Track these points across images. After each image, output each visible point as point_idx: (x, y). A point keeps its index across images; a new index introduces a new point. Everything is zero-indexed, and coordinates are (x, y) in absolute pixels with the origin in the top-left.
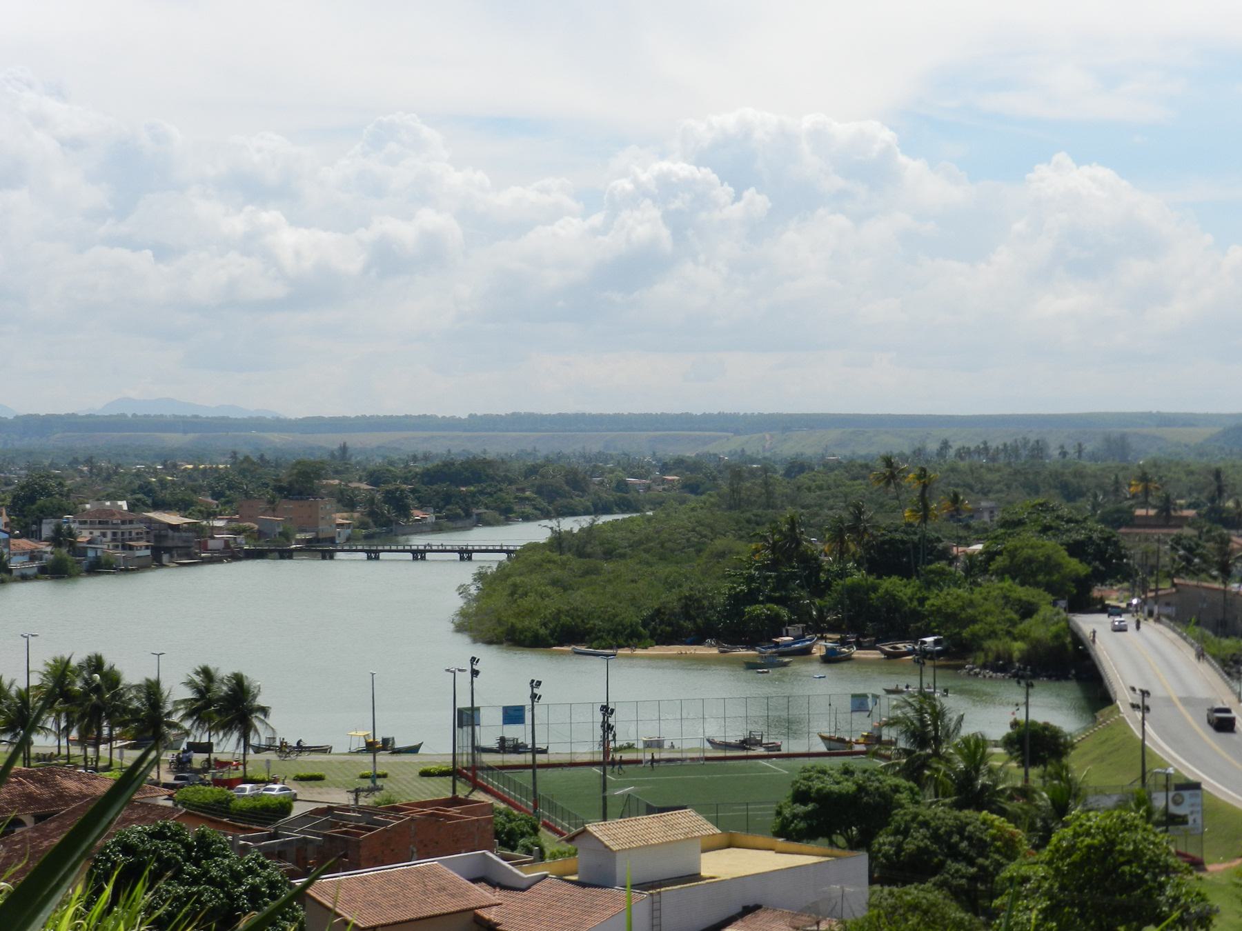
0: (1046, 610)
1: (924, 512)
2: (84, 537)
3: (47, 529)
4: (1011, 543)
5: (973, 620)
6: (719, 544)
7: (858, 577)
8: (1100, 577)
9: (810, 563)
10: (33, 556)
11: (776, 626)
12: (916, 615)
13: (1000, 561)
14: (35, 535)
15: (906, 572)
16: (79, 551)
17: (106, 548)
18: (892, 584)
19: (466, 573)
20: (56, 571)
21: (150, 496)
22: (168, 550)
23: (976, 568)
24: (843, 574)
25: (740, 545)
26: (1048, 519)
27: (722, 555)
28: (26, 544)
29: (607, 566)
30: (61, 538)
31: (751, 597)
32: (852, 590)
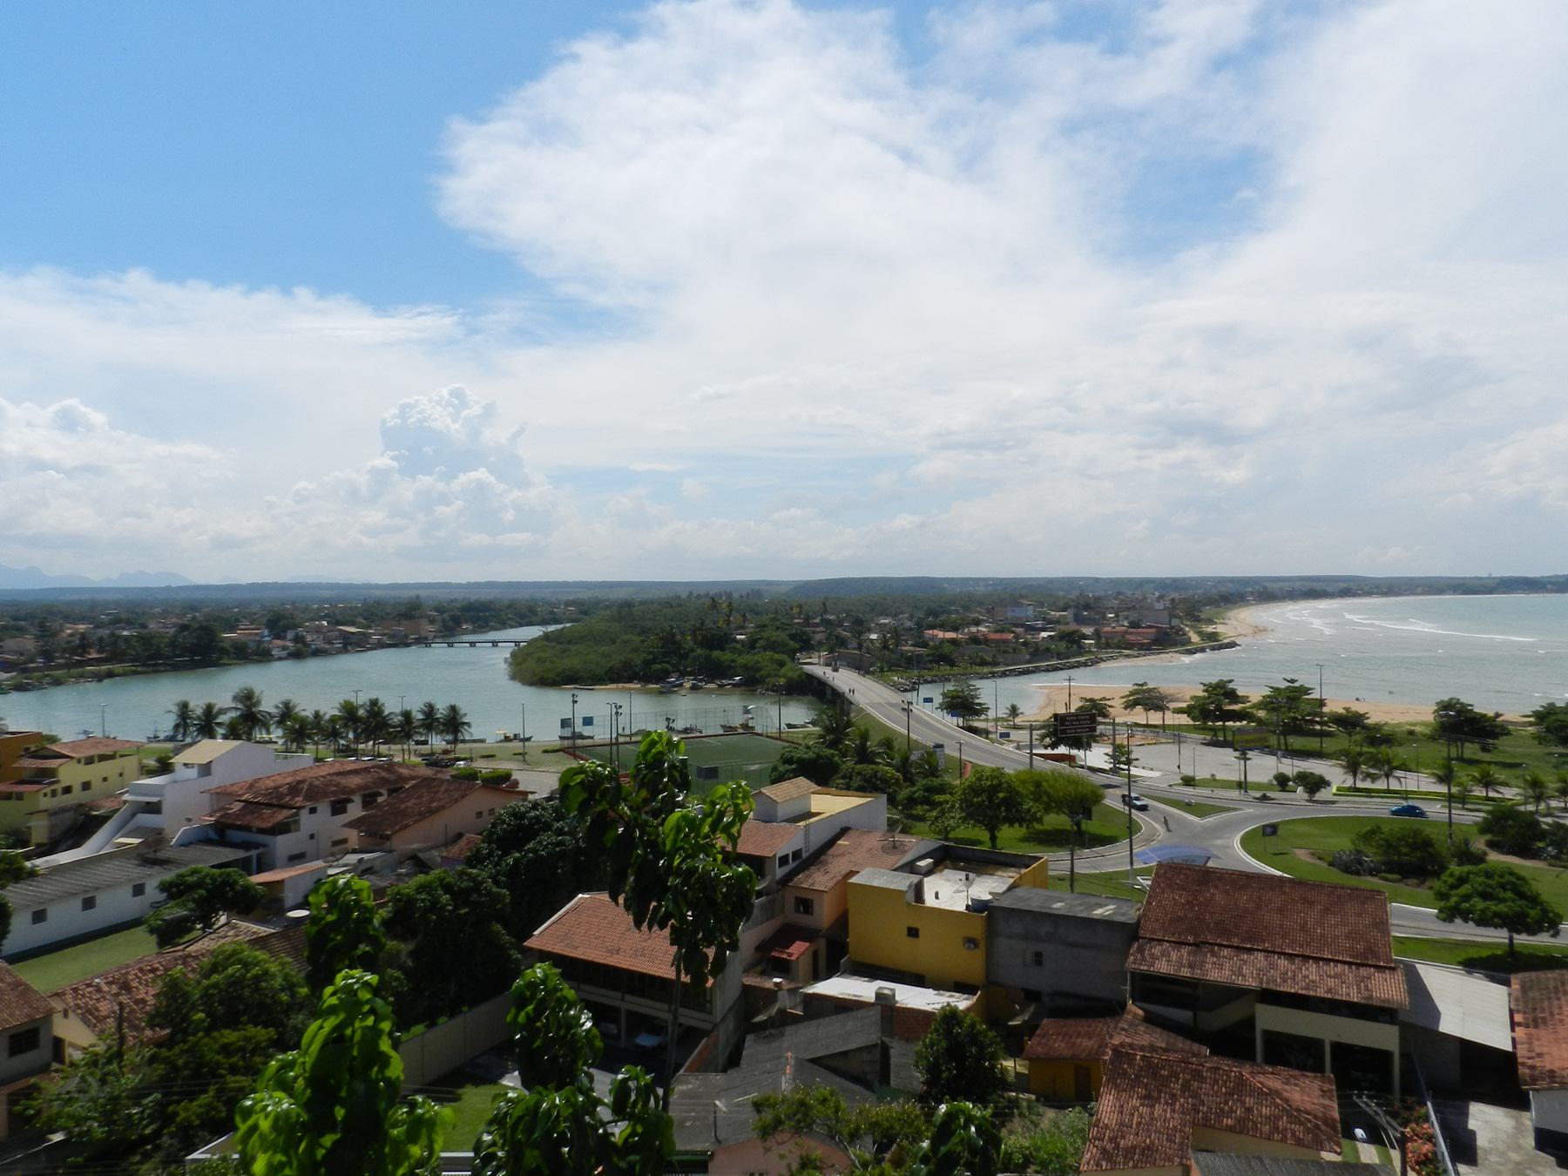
2: (309, 638)
3: (290, 634)
5: (759, 670)
8: (801, 650)
10: (284, 648)
11: (667, 674)
12: (730, 667)
14: (283, 638)
16: (309, 646)
17: (320, 644)
19: (505, 652)
20: (297, 655)
21: (335, 621)
22: (351, 644)
28: (279, 642)
30: (298, 639)
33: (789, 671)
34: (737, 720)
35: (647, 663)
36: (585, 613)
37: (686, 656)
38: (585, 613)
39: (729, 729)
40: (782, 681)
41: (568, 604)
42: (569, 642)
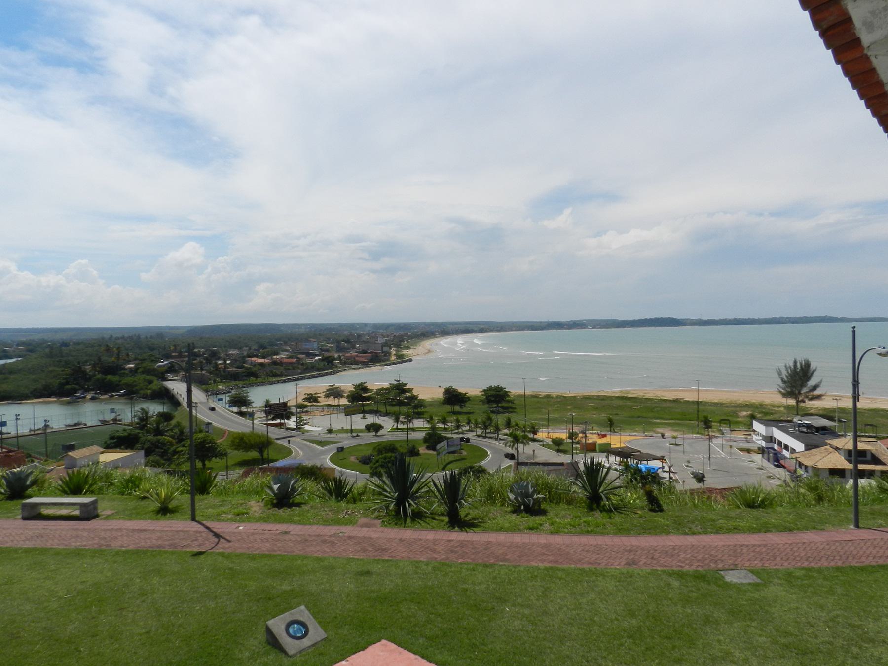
0: (156, 382)
1: (118, 358)
4: (144, 365)
6: (51, 369)
7: (99, 376)
9: (84, 373)
12: (118, 385)
13: (140, 370)
15: (114, 374)
18: (109, 377)
23: (134, 372)
24: (95, 376)
25: (57, 369)
26: (153, 358)
27: (51, 372)
29: (12, 377)
31: (67, 383)
32: (98, 380)
33: (156, 384)
34: (109, 417)
35: (62, 385)
36: (31, 351)
37: (90, 379)
38: (31, 351)
39: (104, 422)
40: (149, 392)
41: (18, 345)
42: (11, 373)
